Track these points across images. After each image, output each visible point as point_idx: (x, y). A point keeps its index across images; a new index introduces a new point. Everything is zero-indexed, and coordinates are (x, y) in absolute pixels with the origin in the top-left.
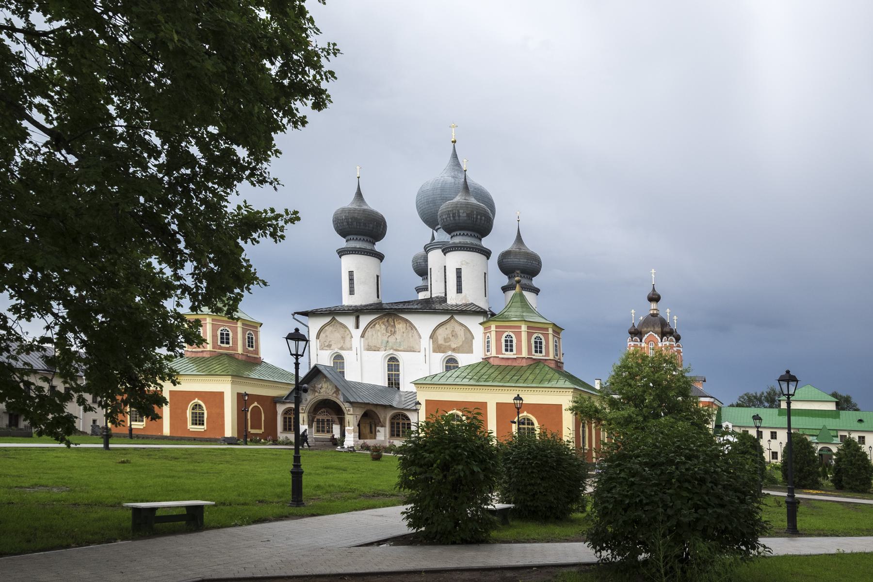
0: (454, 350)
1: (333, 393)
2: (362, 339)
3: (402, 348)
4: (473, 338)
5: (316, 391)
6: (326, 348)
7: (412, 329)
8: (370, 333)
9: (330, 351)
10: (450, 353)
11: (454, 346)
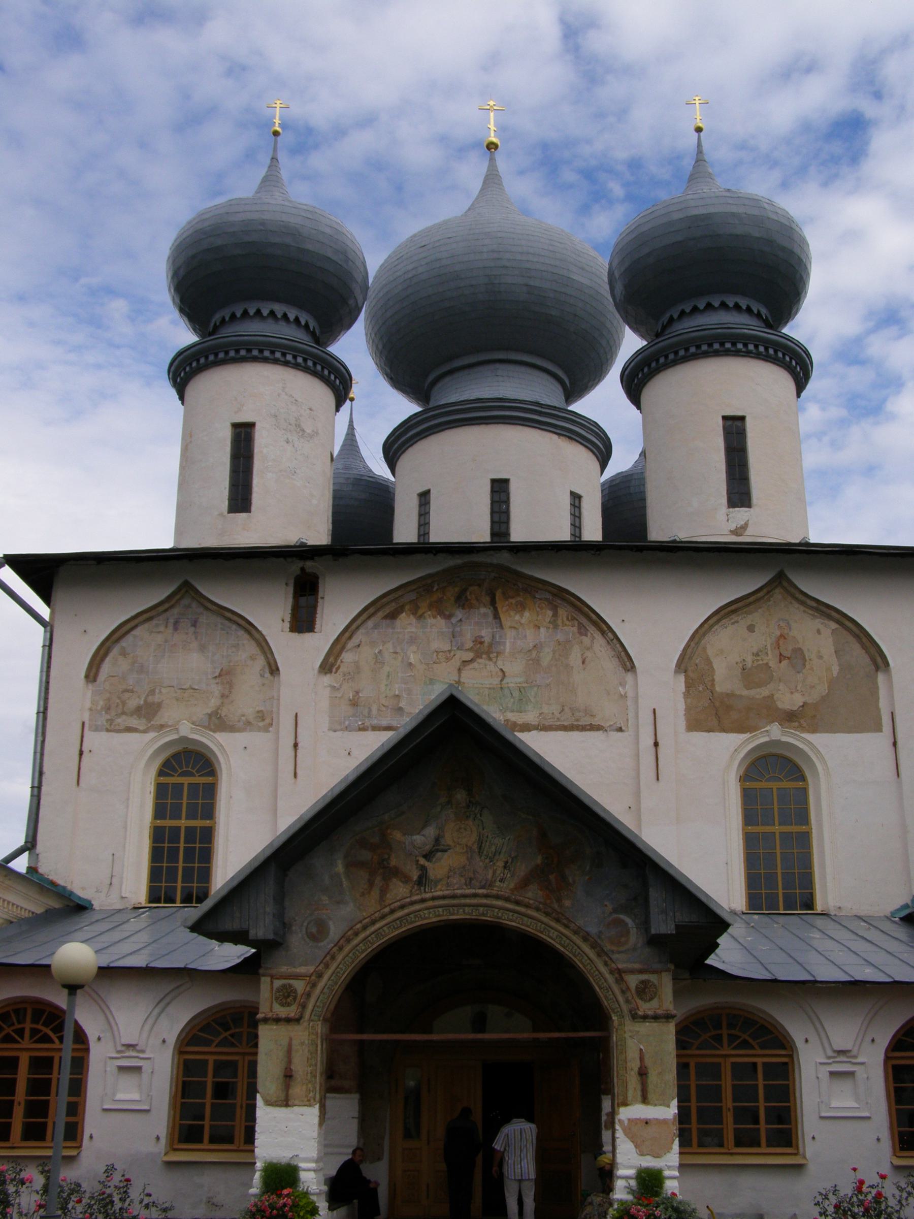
0: (790, 718)
1: (524, 884)
2: (327, 679)
3: (530, 717)
4: (879, 661)
5: (396, 872)
6: (133, 722)
7: (582, 631)
8: (366, 654)
9: (152, 735)
10: (775, 732)
11: (789, 700)
